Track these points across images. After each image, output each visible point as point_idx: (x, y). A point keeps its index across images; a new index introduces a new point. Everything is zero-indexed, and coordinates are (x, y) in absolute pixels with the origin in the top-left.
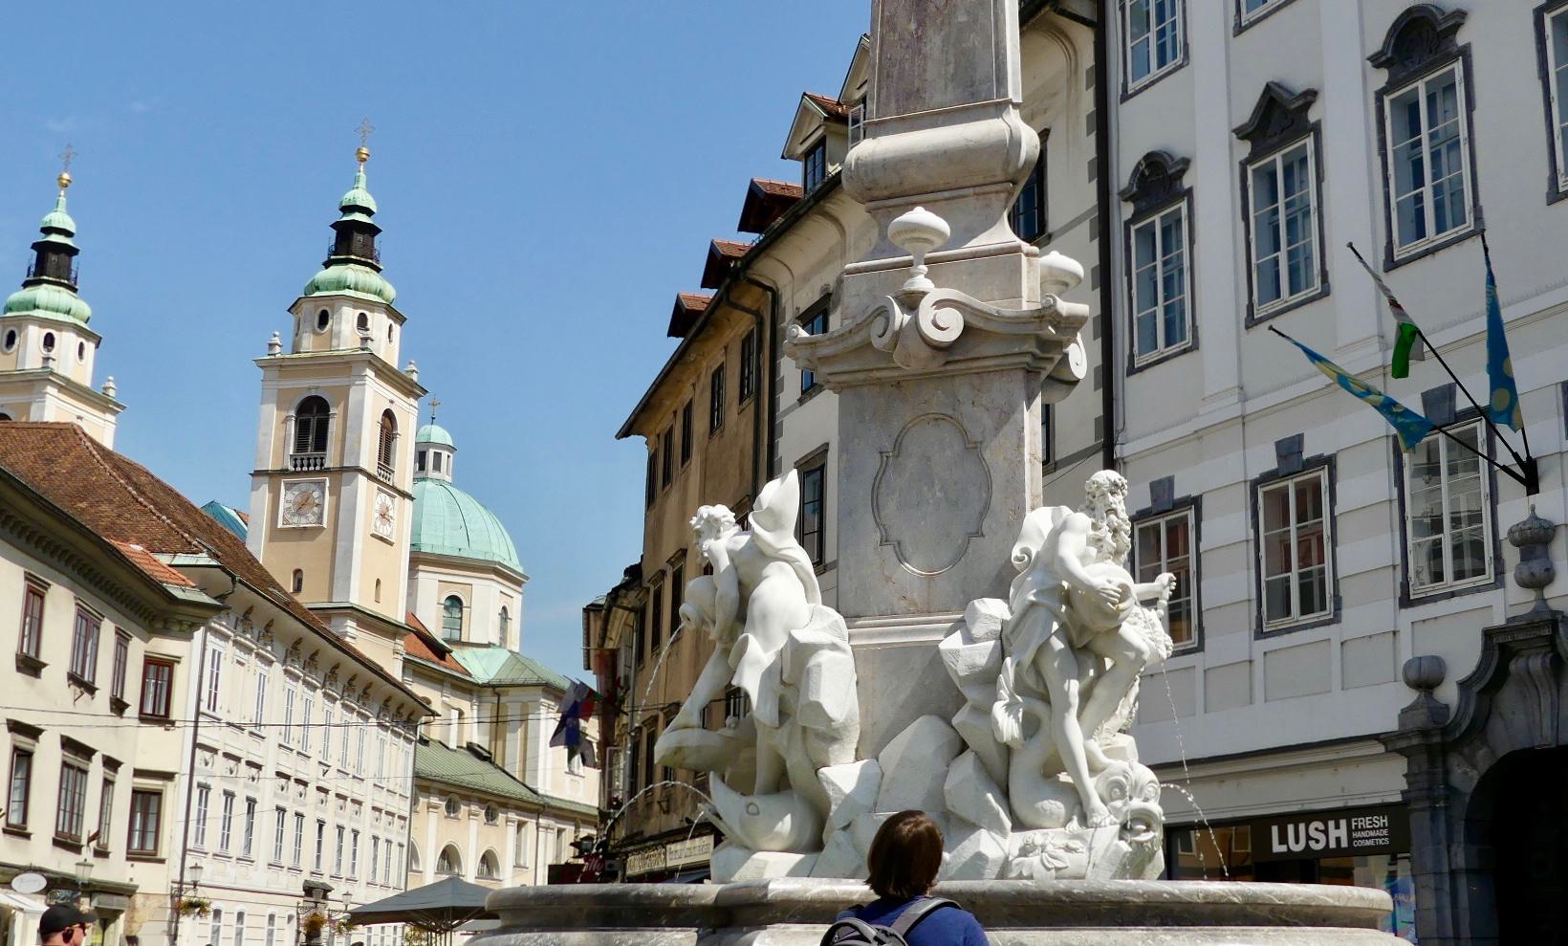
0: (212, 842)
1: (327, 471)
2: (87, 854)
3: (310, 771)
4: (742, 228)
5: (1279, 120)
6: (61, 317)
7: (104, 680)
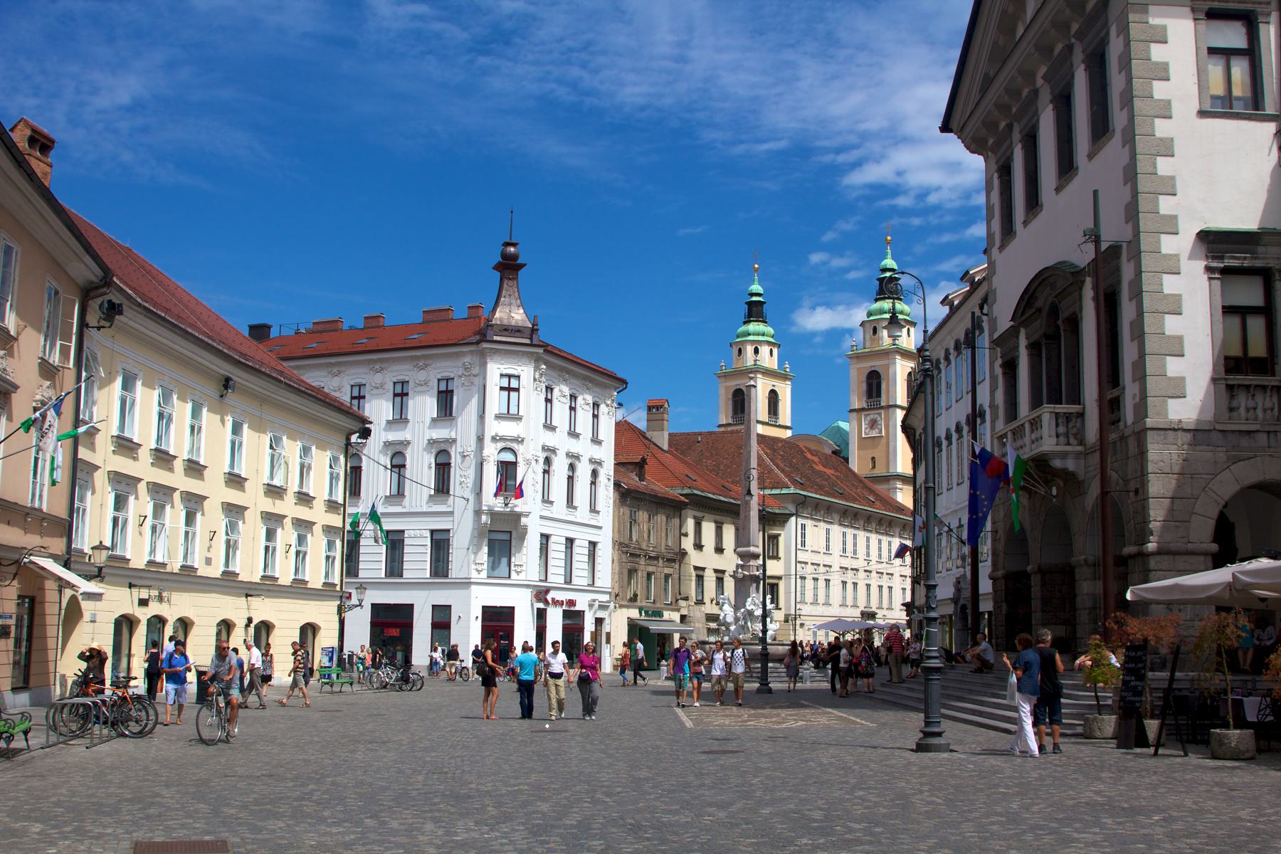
0: (809, 597)
1: (882, 408)
5: (948, 437)
6: (761, 338)
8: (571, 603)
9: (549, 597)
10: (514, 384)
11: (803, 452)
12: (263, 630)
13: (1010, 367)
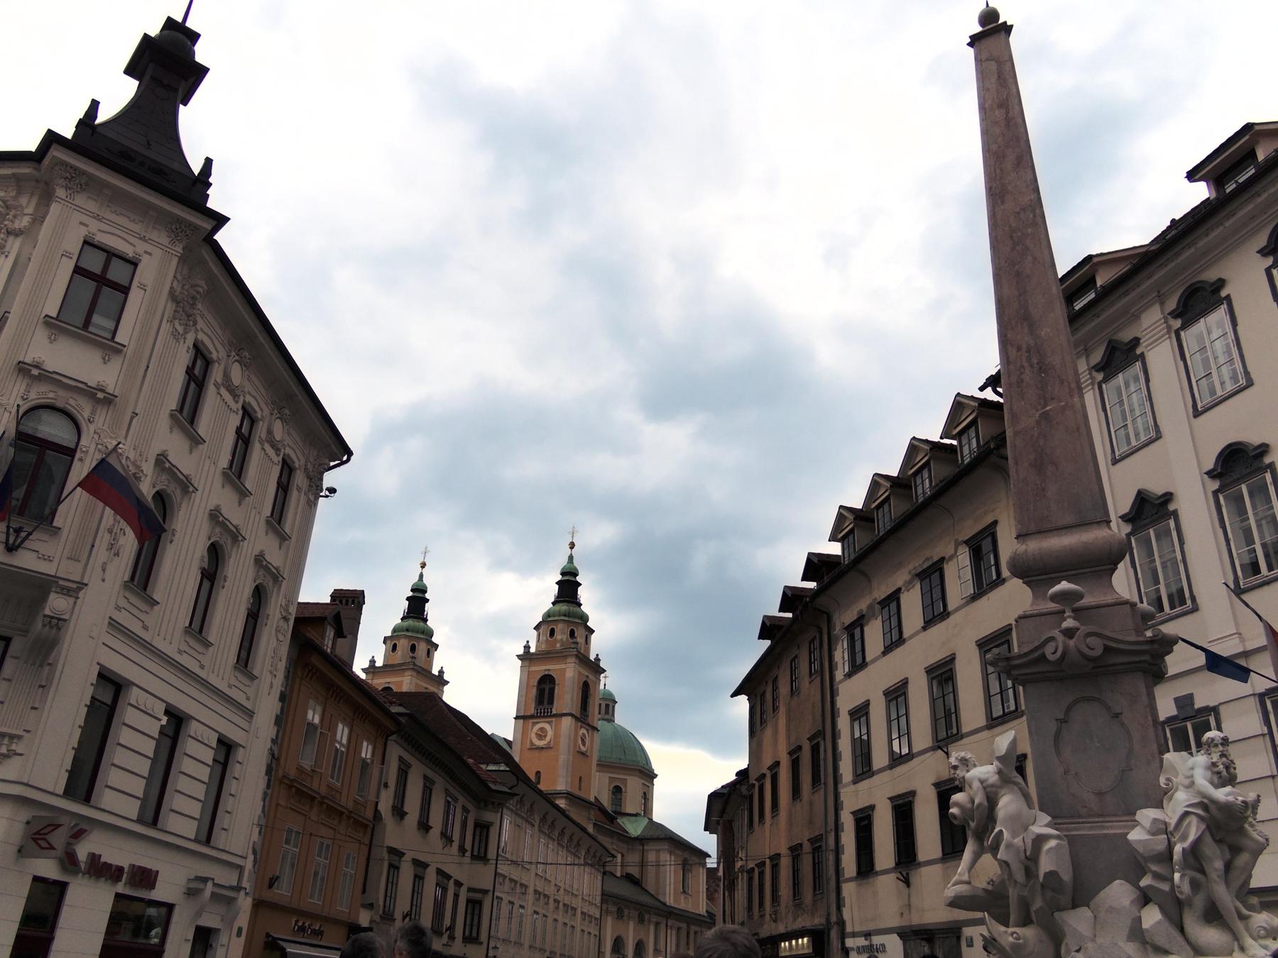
1: (555, 716)
2: (445, 937)
3: (550, 890)
4: (804, 578)
7: (456, 837)
9: (83, 851)
10: (117, 272)
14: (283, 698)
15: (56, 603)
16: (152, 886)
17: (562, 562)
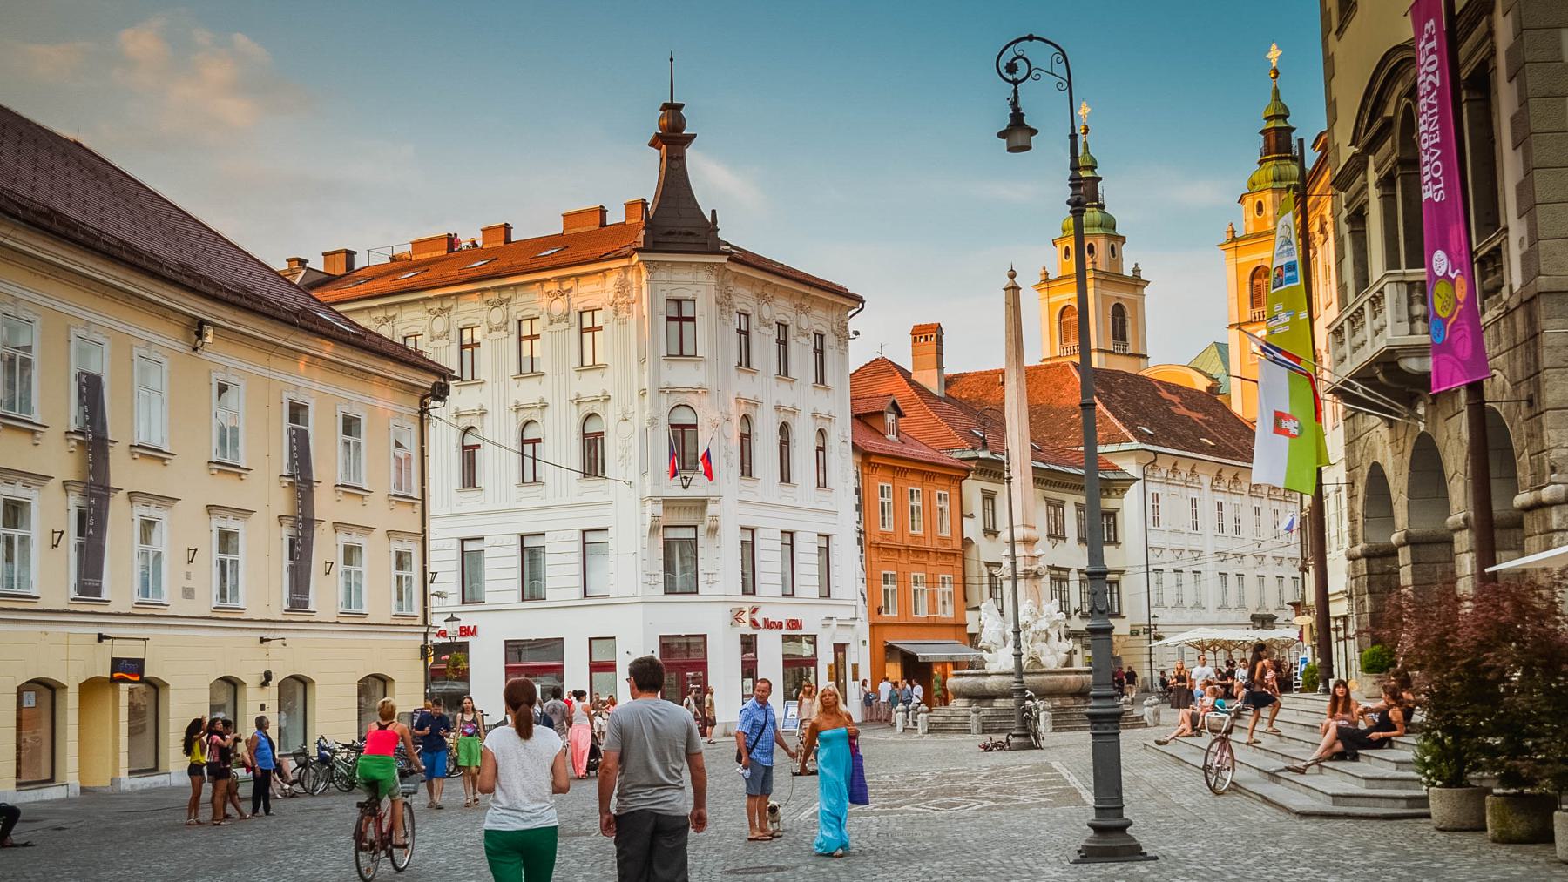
0: (1170, 597)
8: (795, 624)
10: (686, 313)
11: (1155, 389)
12: (296, 689)
13: (1358, 218)
14: (857, 491)
15: (711, 509)
16: (800, 627)
17: (1265, 104)
